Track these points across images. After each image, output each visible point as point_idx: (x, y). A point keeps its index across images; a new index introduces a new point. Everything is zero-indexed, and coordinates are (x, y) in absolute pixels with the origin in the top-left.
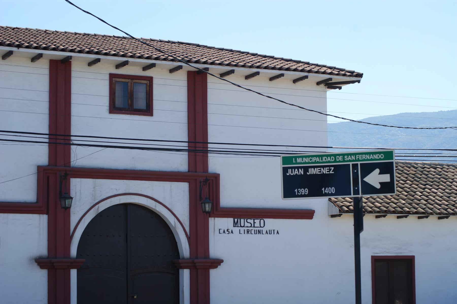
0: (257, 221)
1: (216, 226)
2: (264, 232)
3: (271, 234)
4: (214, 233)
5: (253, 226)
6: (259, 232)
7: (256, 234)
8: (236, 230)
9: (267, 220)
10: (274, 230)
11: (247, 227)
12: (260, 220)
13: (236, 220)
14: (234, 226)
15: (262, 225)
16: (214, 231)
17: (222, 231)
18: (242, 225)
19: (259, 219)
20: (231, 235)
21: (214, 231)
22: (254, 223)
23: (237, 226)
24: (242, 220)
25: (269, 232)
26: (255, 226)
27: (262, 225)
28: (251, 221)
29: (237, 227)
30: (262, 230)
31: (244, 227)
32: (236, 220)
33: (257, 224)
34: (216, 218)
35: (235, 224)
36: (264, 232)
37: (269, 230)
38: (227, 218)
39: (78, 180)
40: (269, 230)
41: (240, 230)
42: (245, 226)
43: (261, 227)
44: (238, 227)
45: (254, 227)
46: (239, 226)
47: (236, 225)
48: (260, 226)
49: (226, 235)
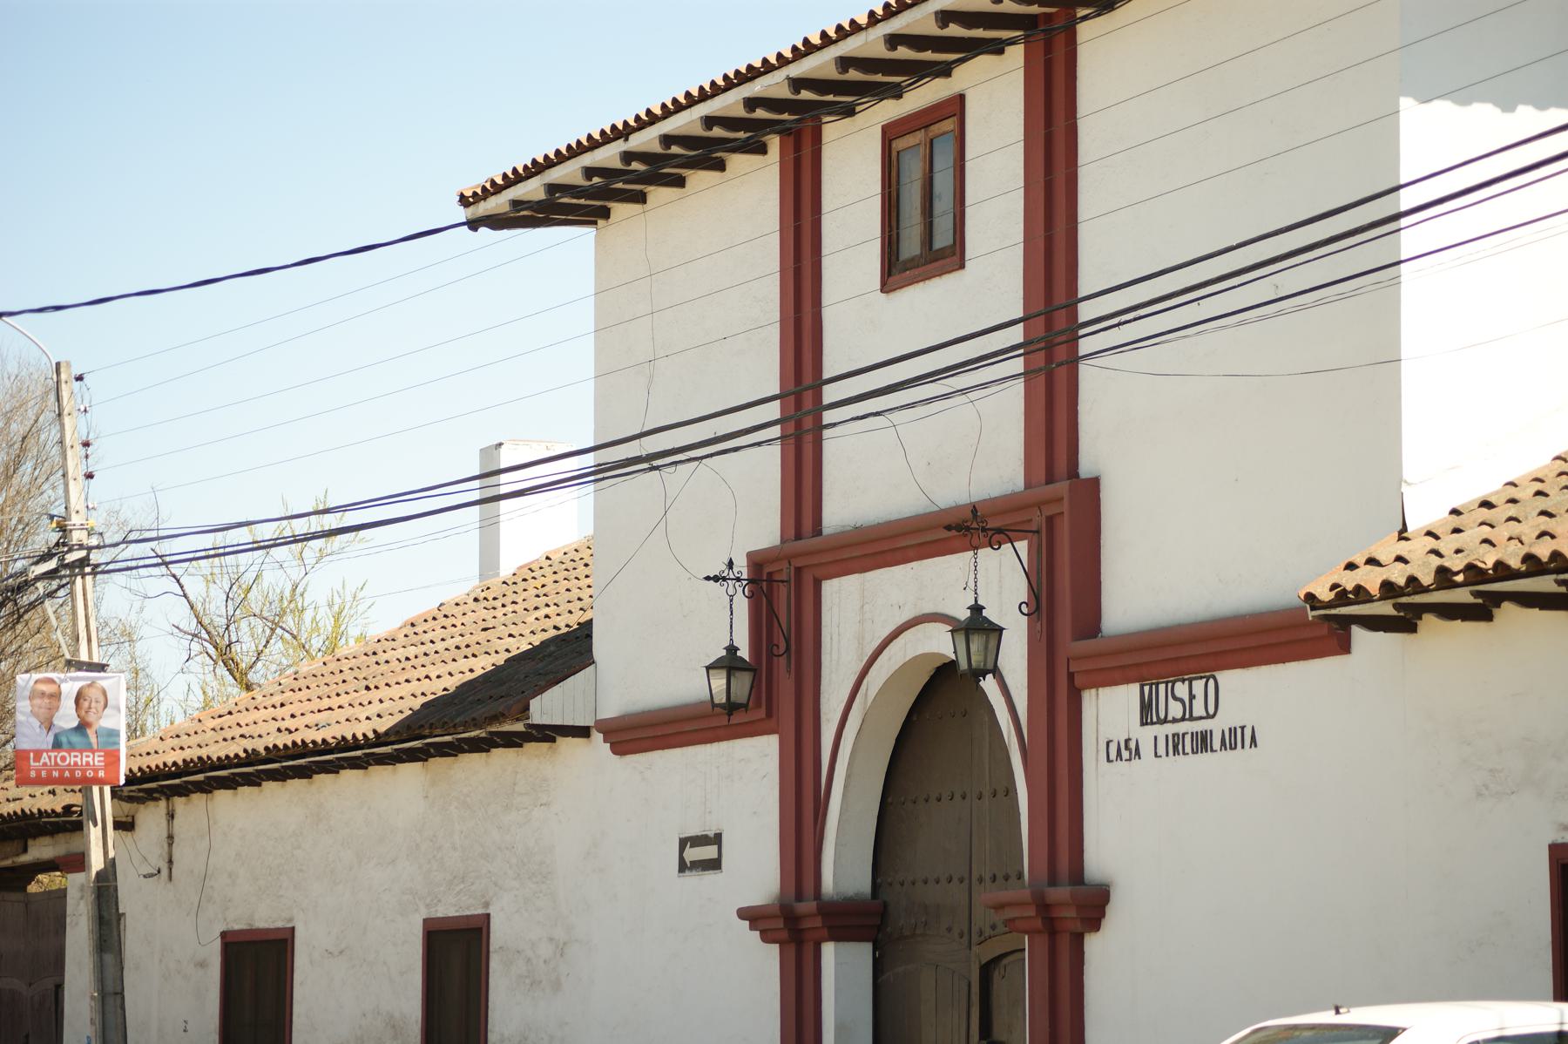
0: (1198, 686)
1: (1101, 728)
2: (1217, 744)
3: (1235, 748)
4: (1097, 760)
5: (1187, 716)
6: (1203, 742)
7: (1197, 752)
8: (1145, 735)
9: (1225, 677)
10: (1243, 728)
11: (1175, 721)
12: (1205, 680)
13: (1147, 689)
14: (1143, 724)
15: (1211, 711)
16: (1098, 751)
17: (1113, 755)
18: (1162, 716)
19: (1201, 678)
20: (1135, 762)
21: (1098, 751)
22: (1192, 697)
23: (1149, 721)
24: (1162, 687)
25: (1234, 739)
26: (1194, 715)
27: (1211, 711)
28: (1181, 689)
29: (1155, 723)
30: (1211, 731)
31: (1165, 721)
32: (1147, 689)
33: (1198, 709)
34: (1101, 689)
35: (1147, 714)
36: (1217, 744)
37: (1167, 736)
38: (1126, 685)
39: (835, 581)
40: (1230, 729)
41: (1156, 738)
42: (1170, 718)
43: (1209, 717)
44: (1152, 723)
45: (1192, 718)
46: (1155, 719)
47: (1147, 720)
48: (1204, 714)
49: (1121, 766)
